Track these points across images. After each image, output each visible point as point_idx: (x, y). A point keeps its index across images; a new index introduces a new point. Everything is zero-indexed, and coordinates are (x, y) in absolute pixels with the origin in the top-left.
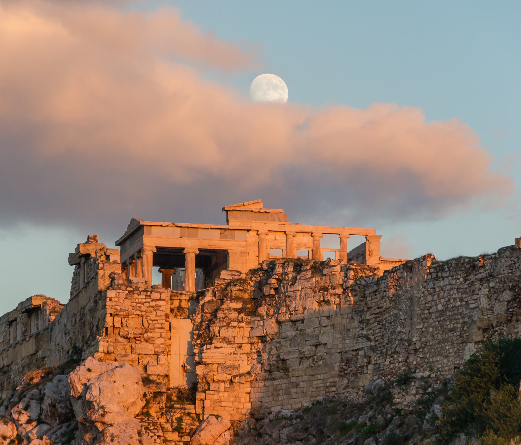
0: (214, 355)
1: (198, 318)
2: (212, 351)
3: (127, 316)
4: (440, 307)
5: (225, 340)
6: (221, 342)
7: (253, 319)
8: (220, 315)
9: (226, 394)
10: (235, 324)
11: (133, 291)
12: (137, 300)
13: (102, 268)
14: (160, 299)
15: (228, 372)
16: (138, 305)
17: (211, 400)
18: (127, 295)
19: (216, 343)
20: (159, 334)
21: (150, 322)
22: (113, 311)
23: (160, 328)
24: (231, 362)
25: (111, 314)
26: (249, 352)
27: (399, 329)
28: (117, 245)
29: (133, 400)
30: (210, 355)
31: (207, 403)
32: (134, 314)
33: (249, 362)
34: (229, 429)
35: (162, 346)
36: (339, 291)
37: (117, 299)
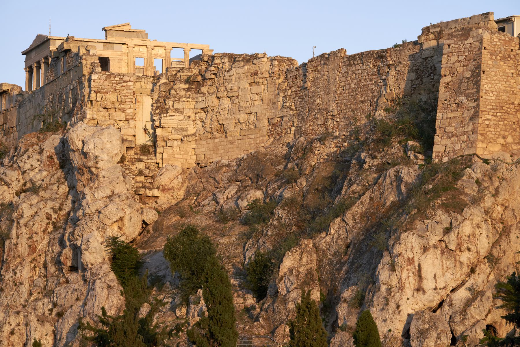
0: (169, 121)
1: (156, 95)
2: (168, 118)
3: (106, 93)
4: (352, 85)
5: (177, 110)
6: (174, 112)
7: (197, 96)
8: (173, 92)
9: (178, 149)
10: (184, 99)
13: (85, 59)
14: (130, 81)
15: (180, 133)
17: (167, 153)
18: (106, 77)
19: (170, 113)
21: (122, 97)
22: (96, 89)
23: (129, 102)
24: (182, 126)
25: (95, 91)
26: (194, 119)
27: (318, 101)
28: (23, 54)
30: (166, 121)
31: (165, 156)
35: (131, 114)
36: (267, 75)
37: (99, 81)
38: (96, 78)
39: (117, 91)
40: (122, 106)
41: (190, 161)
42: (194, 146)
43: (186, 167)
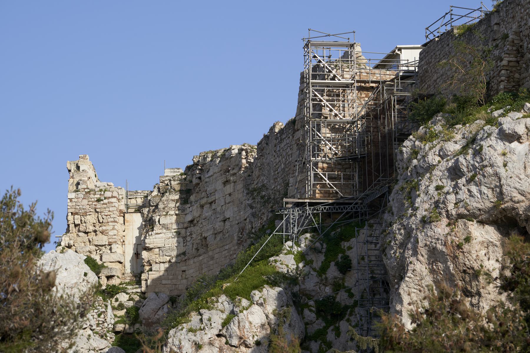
0: (155, 240)
3: (85, 214)
11: (89, 192)
12: (93, 200)
14: (112, 197)
16: (94, 203)
18: (84, 195)
19: (157, 229)
20: (112, 227)
21: (104, 217)
22: (73, 210)
24: (170, 245)
25: (72, 213)
26: (184, 235)
29: (75, 281)
30: (152, 240)
32: (90, 212)
33: (185, 245)
34: (167, 303)
37: (76, 200)
38: (74, 197)
39: (98, 210)
40: (104, 228)
41: (181, 287)
42: (184, 268)
43: (176, 294)
